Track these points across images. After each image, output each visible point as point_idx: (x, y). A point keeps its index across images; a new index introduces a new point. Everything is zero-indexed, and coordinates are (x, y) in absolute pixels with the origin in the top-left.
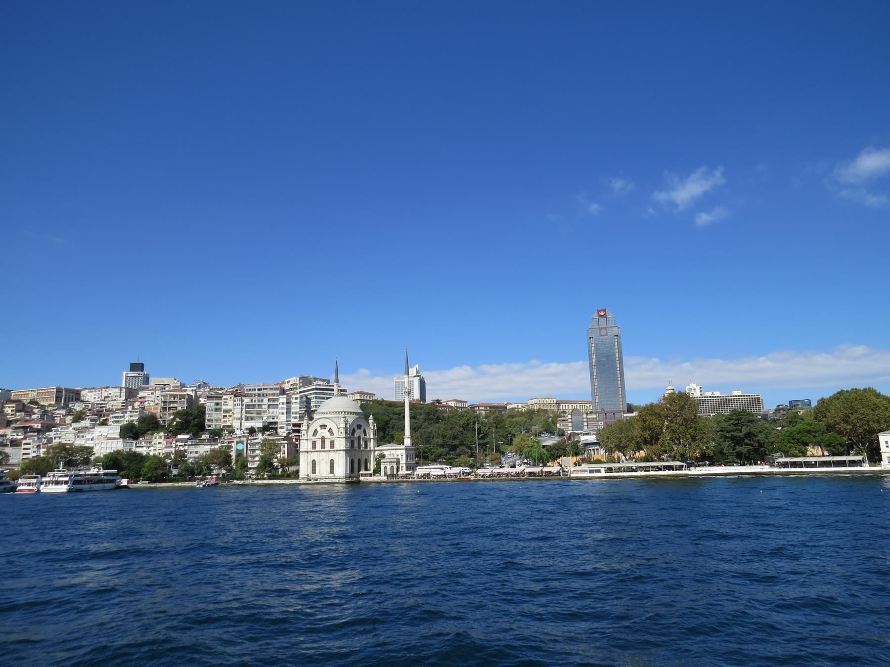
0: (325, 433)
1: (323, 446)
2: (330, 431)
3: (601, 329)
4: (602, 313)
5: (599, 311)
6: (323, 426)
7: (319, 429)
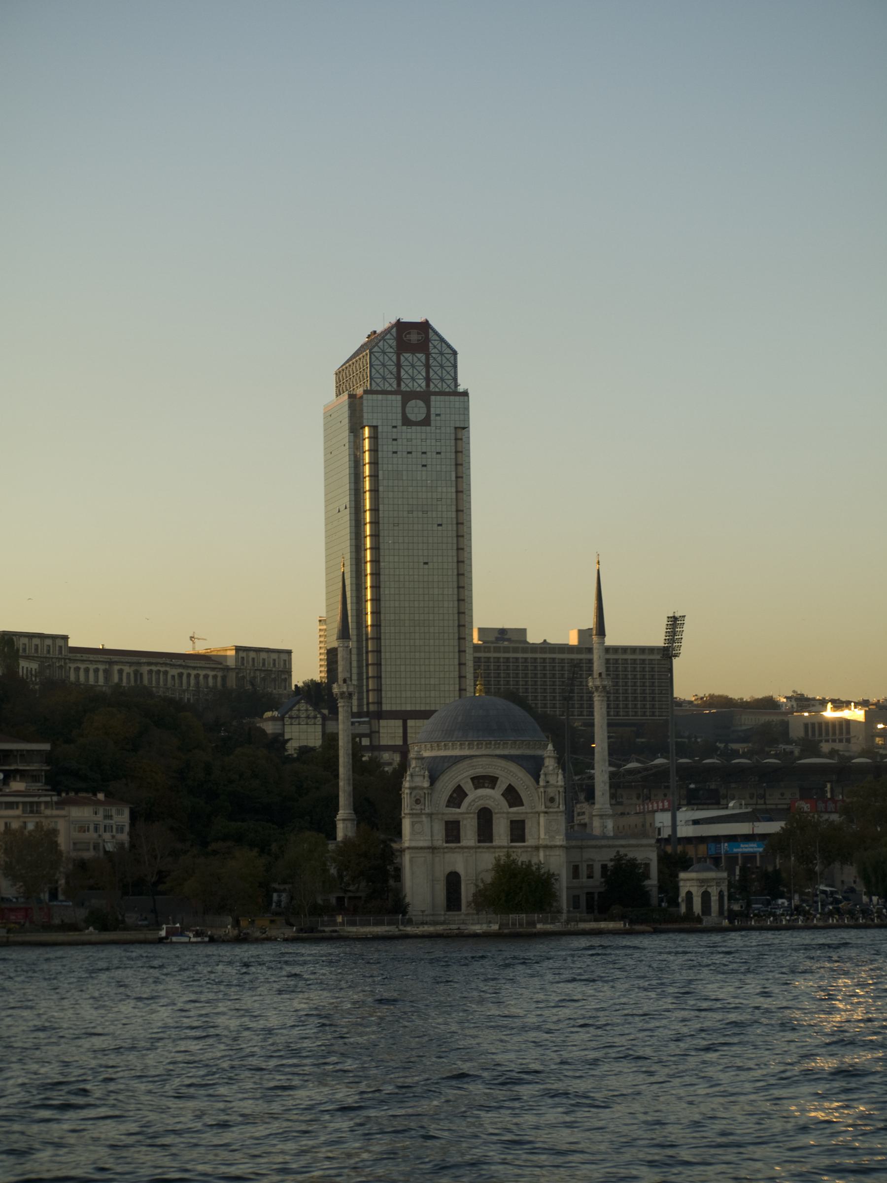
0: (493, 797)
1: (485, 832)
2: (512, 796)
3: (407, 397)
4: (414, 337)
5: (401, 326)
6: (483, 781)
7: (468, 787)
